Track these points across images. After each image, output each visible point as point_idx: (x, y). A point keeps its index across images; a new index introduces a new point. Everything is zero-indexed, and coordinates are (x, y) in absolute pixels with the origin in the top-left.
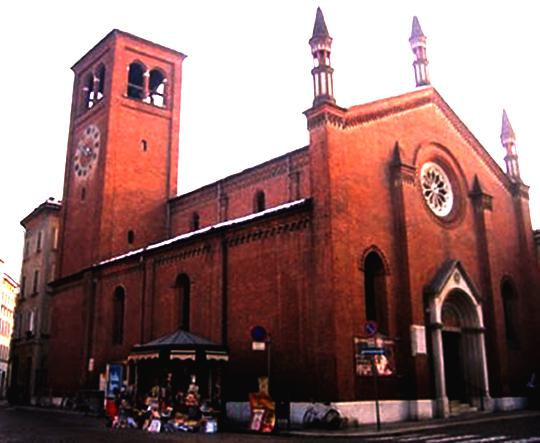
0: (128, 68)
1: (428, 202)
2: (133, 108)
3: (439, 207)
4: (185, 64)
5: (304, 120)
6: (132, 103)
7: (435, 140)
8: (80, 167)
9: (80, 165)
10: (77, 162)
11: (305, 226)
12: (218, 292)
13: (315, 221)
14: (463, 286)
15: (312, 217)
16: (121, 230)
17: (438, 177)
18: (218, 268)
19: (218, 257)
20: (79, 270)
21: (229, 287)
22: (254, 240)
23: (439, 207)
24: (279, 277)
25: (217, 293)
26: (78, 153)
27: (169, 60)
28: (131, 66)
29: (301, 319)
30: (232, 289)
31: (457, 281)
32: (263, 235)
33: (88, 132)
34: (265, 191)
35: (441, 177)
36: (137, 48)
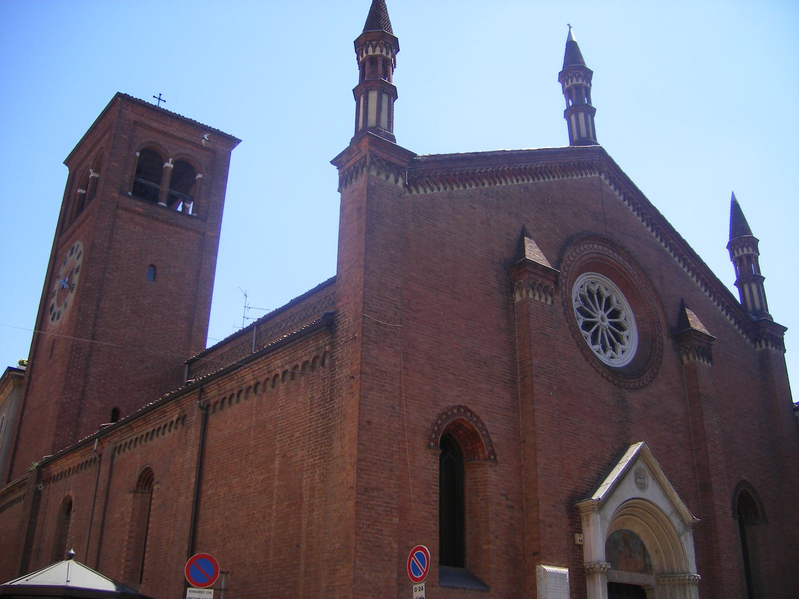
0: (138, 154)
1: (589, 342)
2: (139, 214)
3: (610, 352)
4: (236, 154)
5: (334, 174)
8: (56, 309)
10: (54, 301)
11: (323, 364)
15: (333, 345)
17: (608, 300)
18: (192, 453)
19: (194, 433)
21: (204, 487)
22: (246, 398)
23: (610, 352)
25: (186, 500)
26: (57, 287)
28: (142, 152)
29: (303, 547)
30: (208, 490)
31: (642, 486)
32: (260, 388)
35: (614, 300)
36: (154, 124)
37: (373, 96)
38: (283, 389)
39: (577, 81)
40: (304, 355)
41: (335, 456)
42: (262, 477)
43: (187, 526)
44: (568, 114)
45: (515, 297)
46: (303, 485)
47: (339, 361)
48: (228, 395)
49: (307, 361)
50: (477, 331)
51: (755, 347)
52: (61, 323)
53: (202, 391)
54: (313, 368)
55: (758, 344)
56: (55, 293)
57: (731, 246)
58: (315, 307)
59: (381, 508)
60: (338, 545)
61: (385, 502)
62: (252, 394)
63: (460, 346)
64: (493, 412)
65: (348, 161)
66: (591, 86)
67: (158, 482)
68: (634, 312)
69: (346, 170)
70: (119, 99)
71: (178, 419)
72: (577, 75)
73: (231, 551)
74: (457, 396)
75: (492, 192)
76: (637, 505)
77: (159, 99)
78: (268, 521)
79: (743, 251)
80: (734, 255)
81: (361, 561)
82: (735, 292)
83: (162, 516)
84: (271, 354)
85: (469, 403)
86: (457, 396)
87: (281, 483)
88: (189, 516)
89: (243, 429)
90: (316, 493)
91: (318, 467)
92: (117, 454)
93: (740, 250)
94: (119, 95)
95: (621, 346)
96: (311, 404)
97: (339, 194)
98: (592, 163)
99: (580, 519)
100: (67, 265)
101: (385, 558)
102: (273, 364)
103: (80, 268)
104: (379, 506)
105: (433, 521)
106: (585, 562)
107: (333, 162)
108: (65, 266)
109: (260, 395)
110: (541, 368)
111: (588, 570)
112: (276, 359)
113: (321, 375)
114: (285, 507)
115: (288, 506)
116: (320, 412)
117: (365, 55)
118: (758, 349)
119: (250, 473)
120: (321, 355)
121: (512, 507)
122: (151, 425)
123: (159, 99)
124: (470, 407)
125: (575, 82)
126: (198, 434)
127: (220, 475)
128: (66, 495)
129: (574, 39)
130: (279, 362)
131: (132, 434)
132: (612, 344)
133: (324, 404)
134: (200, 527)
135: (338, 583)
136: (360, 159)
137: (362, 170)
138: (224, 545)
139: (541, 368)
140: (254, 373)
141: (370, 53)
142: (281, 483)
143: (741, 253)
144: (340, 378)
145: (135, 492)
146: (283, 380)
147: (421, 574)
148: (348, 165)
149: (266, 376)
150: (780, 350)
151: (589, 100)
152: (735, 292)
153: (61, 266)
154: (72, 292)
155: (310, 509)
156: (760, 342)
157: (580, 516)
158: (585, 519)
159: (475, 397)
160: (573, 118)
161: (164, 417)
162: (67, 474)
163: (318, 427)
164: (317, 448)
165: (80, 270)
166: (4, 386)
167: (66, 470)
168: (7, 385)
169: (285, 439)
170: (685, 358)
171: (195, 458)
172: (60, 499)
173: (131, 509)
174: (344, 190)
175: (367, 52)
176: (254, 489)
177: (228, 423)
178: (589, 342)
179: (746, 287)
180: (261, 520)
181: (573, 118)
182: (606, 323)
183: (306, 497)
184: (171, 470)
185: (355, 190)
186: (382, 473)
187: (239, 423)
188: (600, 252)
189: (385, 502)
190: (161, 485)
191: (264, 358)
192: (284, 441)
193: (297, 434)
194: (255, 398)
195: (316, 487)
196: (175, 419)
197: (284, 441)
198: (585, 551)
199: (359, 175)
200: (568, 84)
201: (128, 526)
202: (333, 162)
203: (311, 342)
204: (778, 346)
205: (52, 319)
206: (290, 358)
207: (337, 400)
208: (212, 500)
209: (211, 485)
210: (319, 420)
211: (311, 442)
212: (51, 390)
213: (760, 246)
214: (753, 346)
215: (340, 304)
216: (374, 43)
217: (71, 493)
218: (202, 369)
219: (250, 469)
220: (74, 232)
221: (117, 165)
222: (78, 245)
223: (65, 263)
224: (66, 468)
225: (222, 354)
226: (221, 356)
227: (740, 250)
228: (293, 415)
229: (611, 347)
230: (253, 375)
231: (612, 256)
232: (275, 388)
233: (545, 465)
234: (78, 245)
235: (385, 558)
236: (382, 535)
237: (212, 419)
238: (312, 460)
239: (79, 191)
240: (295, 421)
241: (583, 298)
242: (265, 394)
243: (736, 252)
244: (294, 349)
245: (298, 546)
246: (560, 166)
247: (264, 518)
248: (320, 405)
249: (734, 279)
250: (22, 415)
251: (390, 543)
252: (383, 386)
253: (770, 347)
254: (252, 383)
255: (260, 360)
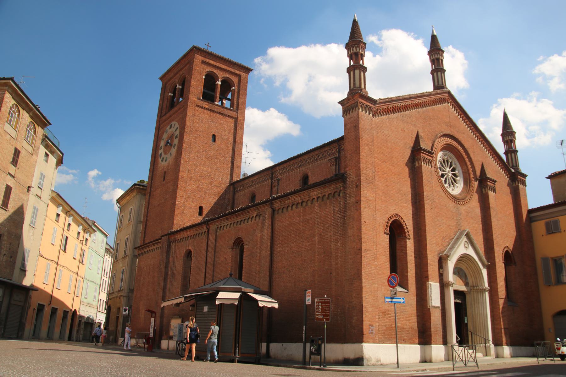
0: (204, 77)
2: (206, 109)
6: (206, 105)
7: (449, 132)
8: (163, 155)
9: (163, 154)
10: (161, 151)
11: (339, 195)
12: (266, 252)
13: (348, 191)
14: (471, 252)
15: (345, 188)
16: (193, 205)
17: (451, 163)
18: (267, 232)
19: (268, 223)
20: (158, 237)
21: (275, 247)
22: (297, 208)
24: (316, 238)
25: (266, 253)
27: (237, 72)
28: (206, 76)
29: (334, 273)
32: (304, 204)
33: (171, 127)
34: (309, 174)
35: (453, 163)
36: (212, 62)
37: (357, 72)
38: (317, 205)
39: (437, 56)
40: (328, 190)
41: (349, 236)
42: (308, 244)
43: (267, 265)
44: (432, 73)
45: (415, 164)
46: (332, 247)
47: (349, 194)
48: (286, 206)
49: (331, 194)
50: (401, 180)
51: (513, 184)
52: (169, 164)
53: (272, 204)
54: (334, 196)
55: (514, 183)
56: (161, 147)
57: (503, 135)
58: (306, 161)
59: (371, 258)
60: (353, 274)
61: (372, 256)
62: (299, 206)
63: (395, 187)
64: (408, 216)
65: (347, 103)
66: (443, 58)
67: (247, 244)
68: (462, 169)
69: (347, 107)
70: (194, 49)
71: (256, 216)
72: (437, 53)
73: (293, 275)
74: (395, 209)
75: (405, 115)
76: (464, 257)
77: (208, 46)
78: (313, 263)
79: (509, 138)
80: (504, 139)
81: (365, 280)
82: (504, 157)
83: (251, 260)
84: (311, 189)
85: (399, 212)
86: (395, 209)
87: (320, 246)
88: (268, 260)
89: (296, 222)
90: (339, 251)
91: (339, 240)
92: (218, 230)
93: (507, 137)
94: (194, 47)
95: (457, 185)
96: (334, 213)
97: (343, 118)
98: (445, 98)
99: (442, 263)
100: (168, 133)
101: (373, 279)
102: (311, 194)
103: (178, 136)
104: (370, 257)
105: (387, 263)
106: (444, 281)
107: (339, 103)
108: (167, 134)
109: (305, 207)
110: (428, 196)
111: (445, 284)
112: (313, 191)
113: (338, 200)
114: (323, 257)
115: (324, 256)
116: (339, 216)
117: (352, 51)
118: (514, 185)
119: (301, 242)
120: (338, 191)
122: (239, 218)
123: (208, 46)
124: (399, 214)
125: (436, 57)
126: (270, 223)
127: (284, 242)
128: (187, 249)
129: (435, 33)
130: (315, 193)
131: (229, 221)
132: (453, 184)
133: (340, 213)
134: (274, 265)
135: (354, 289)
136: (354, 103)
137: (355, 108)
138: (289, 273)
139: (428, 196)
140: (301, 197)
141: (355, 51)
142: (320, 246)
143: (507, 139)
144: (350, 202)
145: (232, 248)
146: (317, 201)
147: (394, 285)
148: (347, 105)
149: (308, 199)
150: (524, 186)
151: (443, 66)
152: (504, 157)
153: (163, 133)
154: (174, 148)
155: (336, 258)
156: (515, 182)
157: (442, 261)
158: (444, 262)
159: (401, 210)
160: (435, 74)
161: (248, 214)
162: (187, 239)
163: (338, 223)
164: (338, 232)
165: (178, 137)
166: (130, 193)
167: (186, 237)
168: (133, 192)
169: (320, 227)
170: (483, 190)
171: (270, 234)
172: (183, 251)
173: (231, 256)
174: (345, 116)
175: (353, 50)
176: (304, 249)
177: (287, 219)
178: (444, 182)
179: (509, 155)
180: (309, 262)
181: (435, 74)
182: (450, 174)
183: (334, 253)
184: (254, 239)
185: (352, 117)
186: (371, 243)
187: (293, 219)
188: (449, 141)
189: (372, 256)
190: (249, 245)
191: (307, 191)
192: (320, 228)
193: (327, 226)
194: (302, 208)
195: (339, 249)
196: (255, 215)
197: (320, 228)
198: (444, 276)
199: (354, 110)
200: (433, 57)
201: (230, 264)
202: (339, 103)
203: (333, 185)
204: (523, 184)
205: (162, 161)
206: (321, 191)
207: (349, 212)
208: (280, 253)
209: (279, 246)
210: (338, 220)
211: (335, 229)
212: (167, 197)
213: (517, 135)
214: (512, 183)
215: (347, 169)
216: (356, 46)
217: (190, 248)
218: (241, 187)
219: (301, 240)
220: (170, 116)
221: (195, 83)
222: (175, 124)
223: (166, 132)
224: (186, 236)
225: (253, 180)
226: (252, 181)
227: (507, 137)
228: (324, 217)
229: (452, 185)
230: (300, 198)
231: (453, 143)
232: (313, 204)
233: (430, 239)
234: (175, 124)
235: (373, 279)
236: (372, 269)
237: (276, 216)
238: (336, 237)
239: (170, 94)
240: (325, 220)
241: (441, 163)
242: (307, 207)
243: (505, 138)
244: (323, 188)
245: (331, 273)
246: (432, 101)
247: (311, 261)
248: (339, 213)
249: (504, 151)
250: (148, 208)
251: (375, 273)
252: (369, 206)
253: (519, 184)
254: (300, 201)
255: (305, 191)
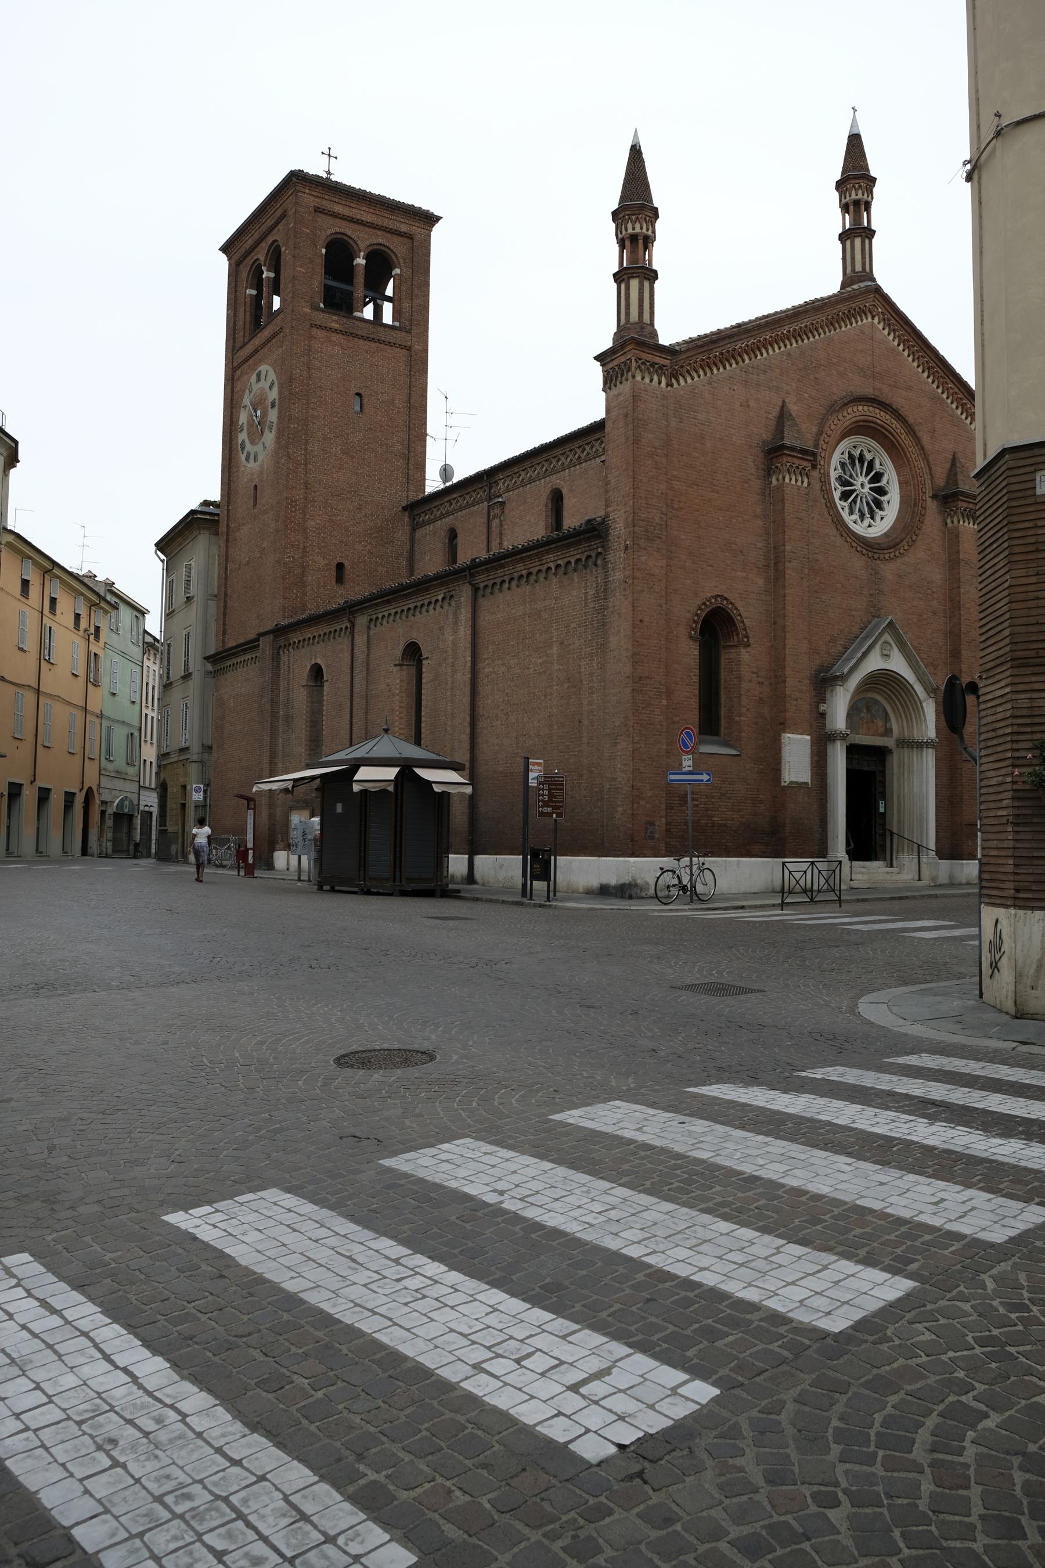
0: (324, 251)
1: (845, 514)
3: (868, 521)
4: (437, 233)
5: (597, 371)
6: (334, 321)
7: (868, 391)
8: (248, 446)
9: (247, 443)
10: (242, 436)
12: (464, 674)
13: (610, 557)
14: (898, 664)
16: (321, 562)
18: (464, 632)
19: (465, 614)
20: (252, 635)
21: (480, 665)
23: (868, 521)
24: (555, 650)
25: (463, 676)
26: (243, 418)
27: (404, 228)
28: (328, 247)
29: (585, 722)
30: (486, 669)
31: (886, 656)
33: (258, 380)
34: (564, 491)
35: (877, 463)
36: (338, 209)
37: (634, 283)
42: (540, 661)
43: (467, 700)
50: (734, 520)
52: (261, 466)
56: (242, 426)
60: (617, 724)
64: (746, 598)
66: (872, 198)
71: (444, 598)
75: (753, 367)
78: (550, 700)
88: (467, 690)
92: (372, 626)
95: (881, 513)
96: (586, 599)
100: (254, 392)
103: (277, 401)
115: (568, 688)
117: (624, 232)
121: (762, 683)
124: (726, 596)
126: (470, 615)
141: (630, 231)
146: (555, 574)
160: (848, 243)
164: (593, 639)
165: (277, 404)
170: (949, 521)
172: (306, 666)
173: (398, 681)
175: (626, 230)
177: (501, 607)
180: (543, 698)
187: (512, 609)
193: (573, 625)
196: (440, 598)
201: (398, 697)
202: (597, 358)
205: (247, 459)
216: (634, 217)
217: (319, 661)
231: (878, 416)
241: (843, 465)
245: (580, 722)
247: (545, 696)
251: (660, 721)
